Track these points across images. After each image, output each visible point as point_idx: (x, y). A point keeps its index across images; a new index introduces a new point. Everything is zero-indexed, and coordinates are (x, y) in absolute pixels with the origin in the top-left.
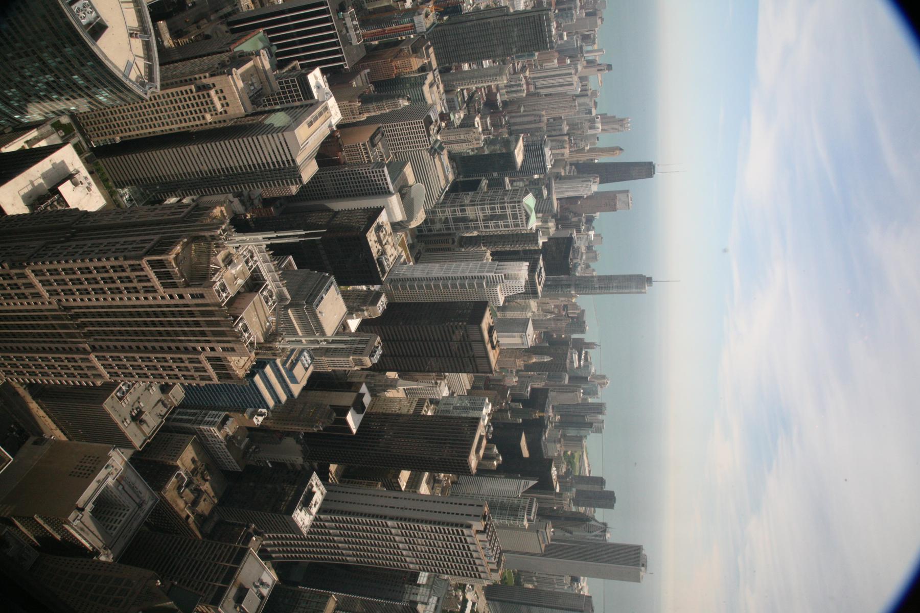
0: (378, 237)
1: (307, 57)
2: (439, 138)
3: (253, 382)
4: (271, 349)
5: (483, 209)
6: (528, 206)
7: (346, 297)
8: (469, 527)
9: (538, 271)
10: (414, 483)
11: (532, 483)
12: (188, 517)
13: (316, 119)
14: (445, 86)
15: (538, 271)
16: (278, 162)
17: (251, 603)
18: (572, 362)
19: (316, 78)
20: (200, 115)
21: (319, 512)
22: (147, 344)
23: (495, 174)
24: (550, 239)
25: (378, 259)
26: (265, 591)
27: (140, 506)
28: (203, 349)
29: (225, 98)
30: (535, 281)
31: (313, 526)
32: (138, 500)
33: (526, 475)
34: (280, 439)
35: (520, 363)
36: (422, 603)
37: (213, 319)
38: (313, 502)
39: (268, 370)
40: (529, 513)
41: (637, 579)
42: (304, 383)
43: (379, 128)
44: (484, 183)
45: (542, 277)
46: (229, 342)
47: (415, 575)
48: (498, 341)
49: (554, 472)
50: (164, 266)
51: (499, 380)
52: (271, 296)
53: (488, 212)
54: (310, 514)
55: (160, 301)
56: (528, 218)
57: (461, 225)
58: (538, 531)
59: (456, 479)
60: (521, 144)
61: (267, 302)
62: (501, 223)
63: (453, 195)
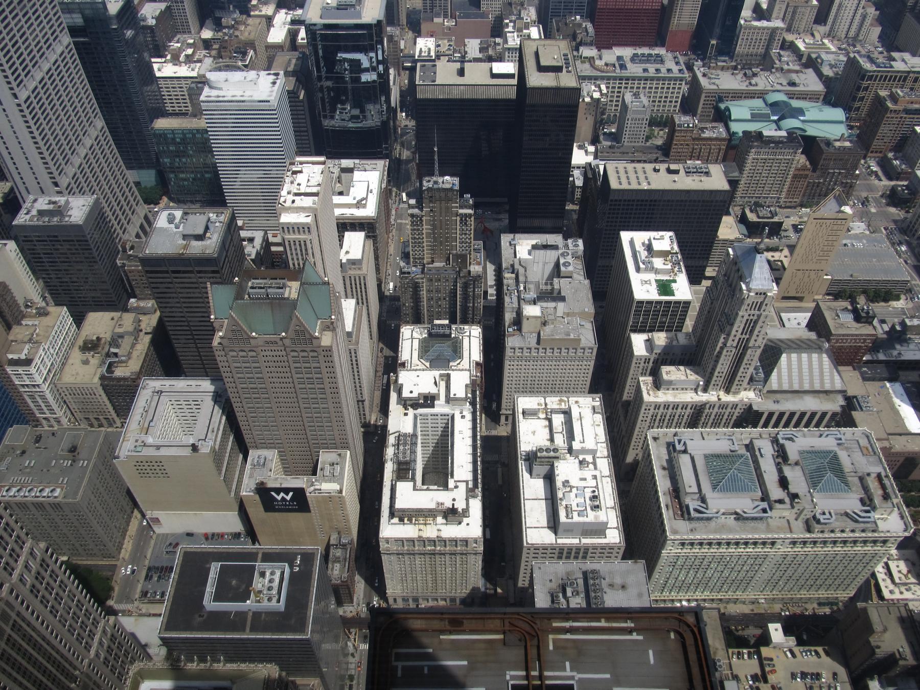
12: (146, 333)
17: (197, 222)
26: (178, 214)
31: (82, 192)
32: (156, 398)
36: (105, 8)
38: (51, 207)
54: (67, 202)
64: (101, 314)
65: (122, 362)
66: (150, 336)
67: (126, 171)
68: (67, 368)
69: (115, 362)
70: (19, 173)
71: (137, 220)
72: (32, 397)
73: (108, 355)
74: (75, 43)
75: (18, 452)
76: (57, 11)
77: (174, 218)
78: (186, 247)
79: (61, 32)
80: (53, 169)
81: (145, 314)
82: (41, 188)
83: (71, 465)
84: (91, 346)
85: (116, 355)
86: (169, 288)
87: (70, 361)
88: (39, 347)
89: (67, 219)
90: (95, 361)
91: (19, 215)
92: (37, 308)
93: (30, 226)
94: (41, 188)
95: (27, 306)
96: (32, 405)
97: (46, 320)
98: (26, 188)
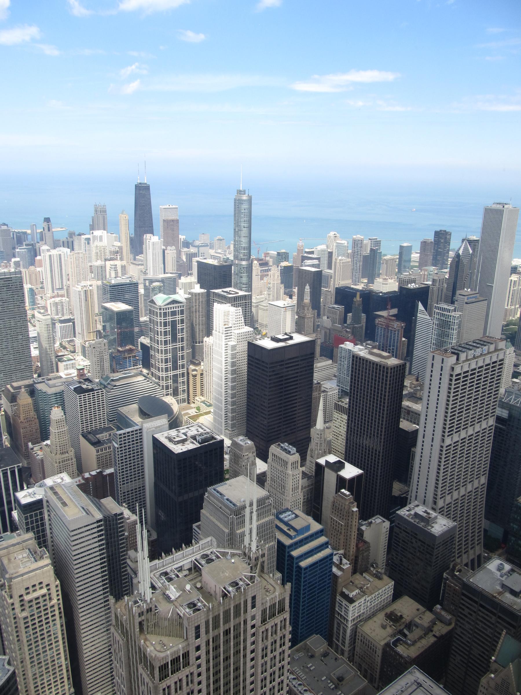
0: (178, 442)
1: (9, 502)
2: (97, 380)
3: (306, 568)
4: (257, 559)
5: (166, 342)
6: (164, 301)
7: (236, 474)
8: (453, 369)
9: (225, 294)
10: (414, 417)
11: (421, 307)
12: (434, 636)
13: (60, 499)
14: (53, 372)
15: (225, 294)
16: (99, 536)
18: (313, 266)
19: (25, 496)
20: (49, 611)
21: (434, 509)
22: (248, 682)
23: (136, 329)
24: (198, 282)
25: (200, 444)
26: (507, 567)
27: (420, 685)
28: (253, 627)
29: (34, 586)
30: (234, 297)
31: (448, 516)
32: (414, 687)
33: (413, 311)
34: (365, 542)
35: (309, 313)
37: (221, 617)
39: (295, 553)
40: (449, 311)
41: (515, 211)
42: (310, 520)
43: (83, 436)
44: (145, 340)
45: (232, 291)
46: (246, 602)
47: (499, 419)
48: (286, 334)
49: (412, 286)
50: (166, 665)
51: (325, 333)
52: (207, 556)
53: (169, 338)
54: (436, 518)
55: (203, 669)
56: (174, 302)
57: (180, 362)
58: (466, 303)
59: (414, 377)
60: (108, 305)
61: (212, 560)
62: (179, 326)
63: (153, 370)
64: (413, 601)
65: (407, 643)
66: (435, 639)
67: (483, 519)
68: (370, 622)
69: (402, 640)
70: (418, 485)
71: (472, 555)
72: (338, 624)
73: (401, 632)
74: (496, 427)
75: (310, 654)
76: (496, 405)
77: (503, 569)
78: (500, 593)
79: (491, 417)
80: (439, 493)
81: (441, 621)
82: (425, 500)
83: (333, 689)
84: (394, 618)
85: (405, 636)
86: (471, 615)
87: (375, 619)
88: (363, 596)
89: (429, 528)
90: (389, 630)
91: (403, 509)
92: (377, 571)
93: (405, 519)
94: (425, 500)
95: (373, 566)
96: (335, 629)
97: (377, 582)
98: (416, 496)
